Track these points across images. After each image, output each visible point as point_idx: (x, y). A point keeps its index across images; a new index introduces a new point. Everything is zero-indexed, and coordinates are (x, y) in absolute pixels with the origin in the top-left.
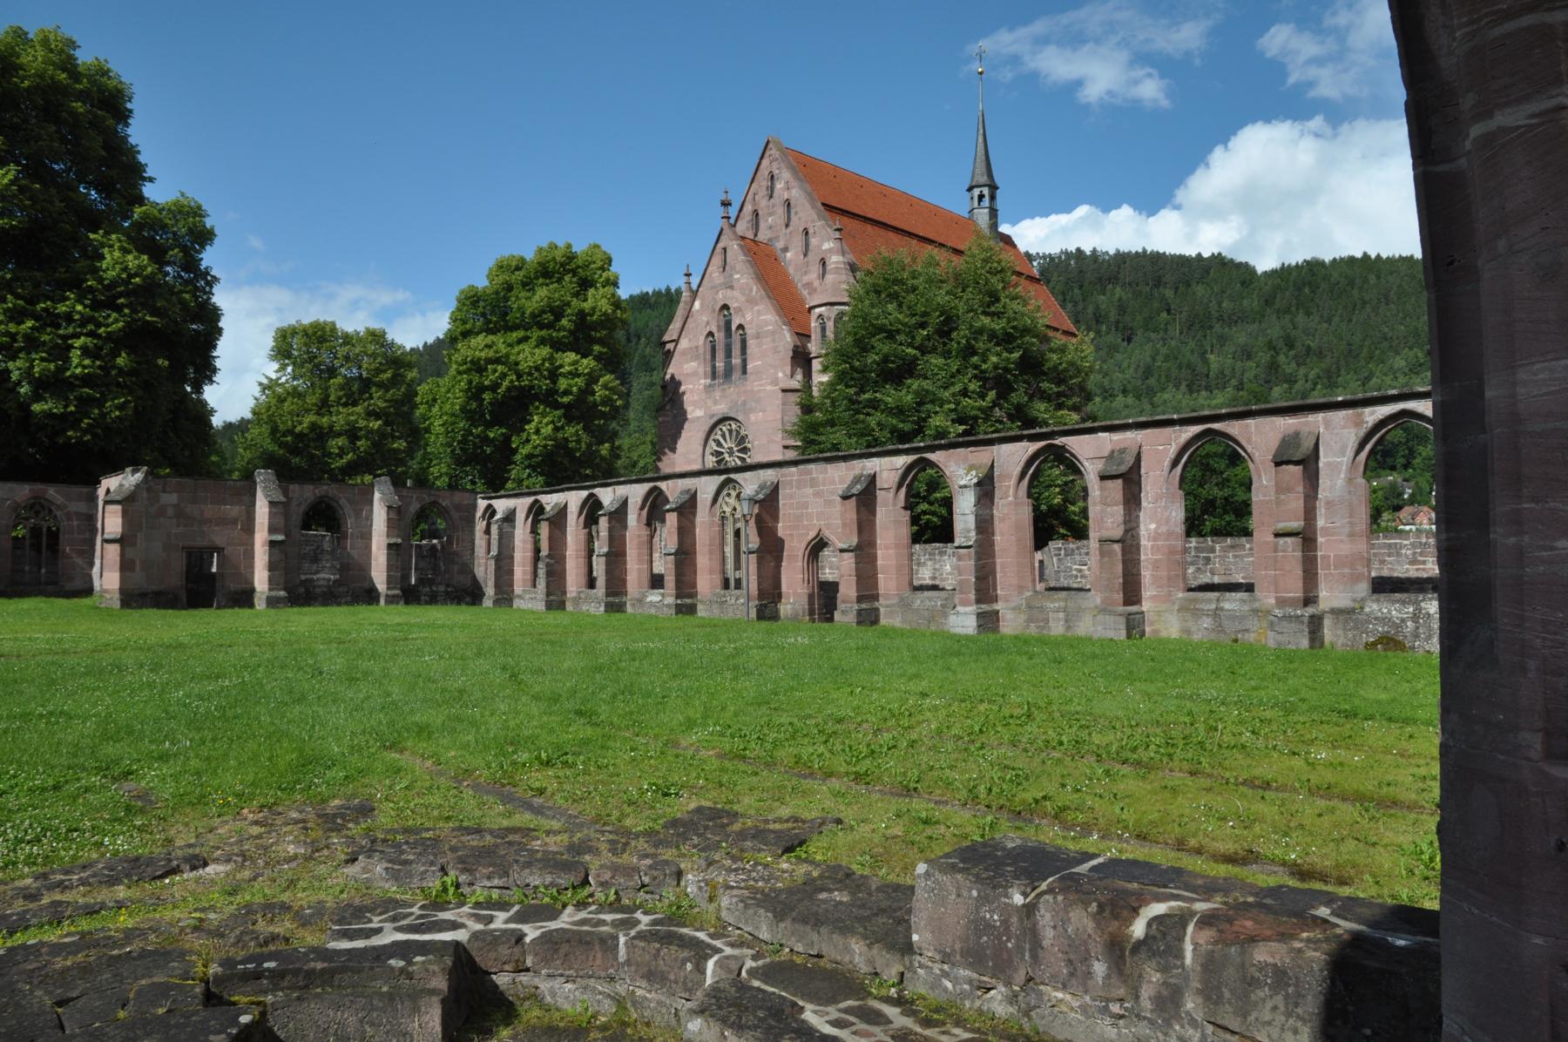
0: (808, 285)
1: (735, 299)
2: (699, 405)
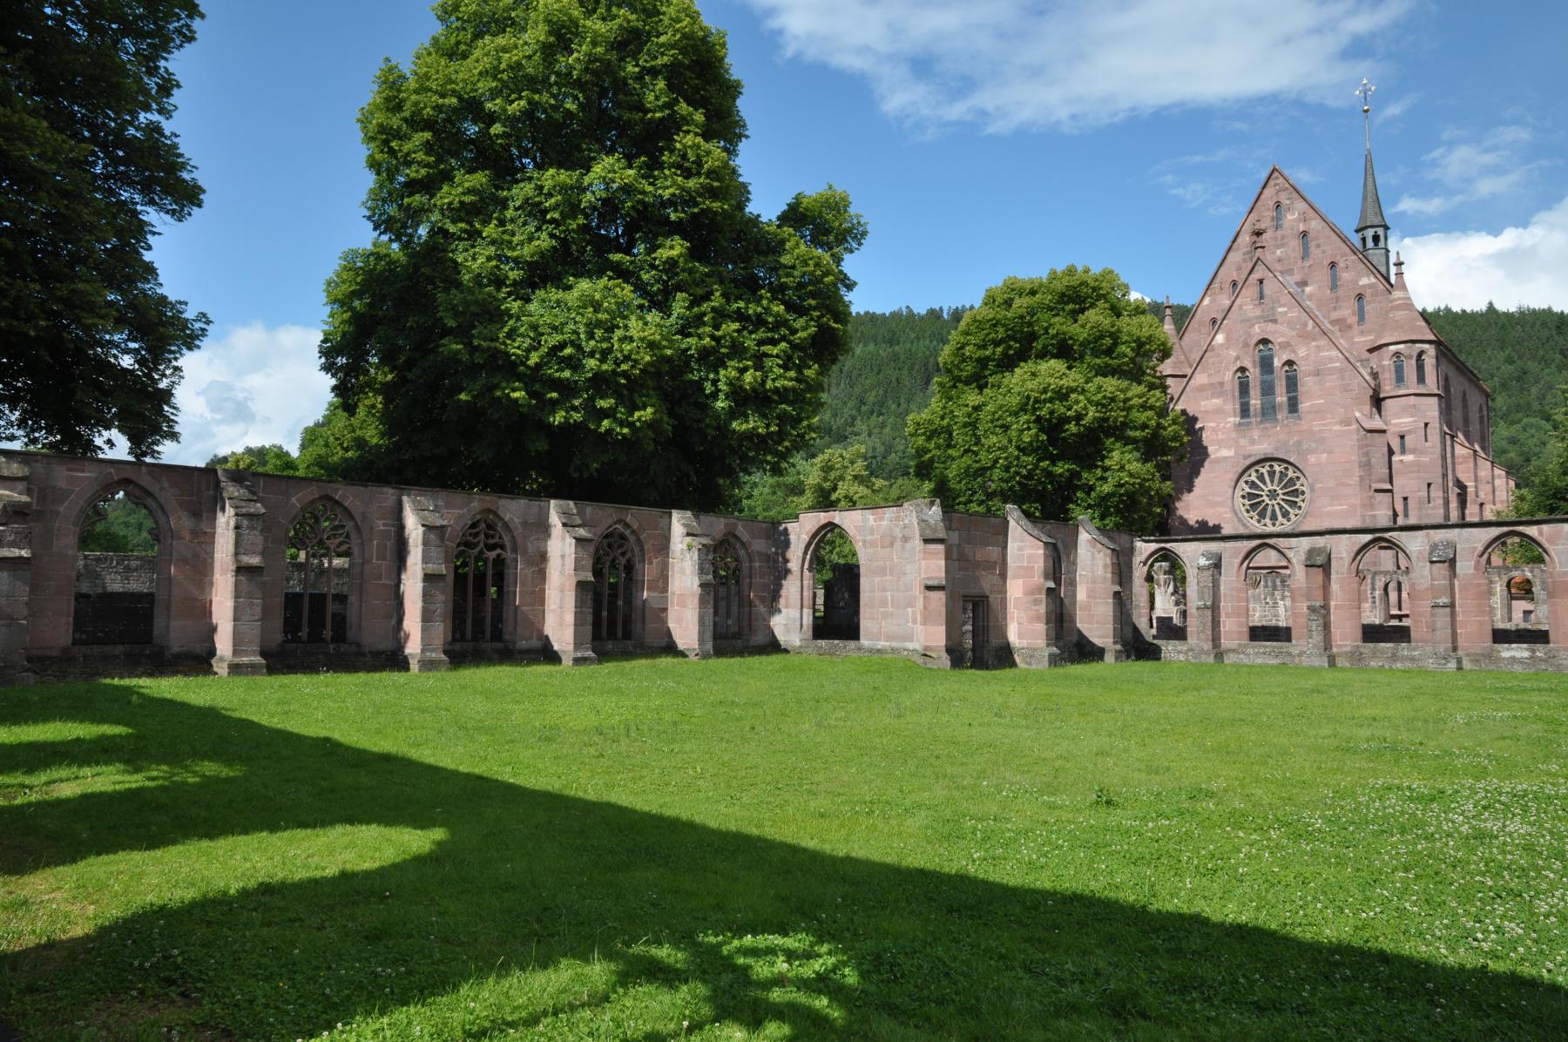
0: (1340, 323)
2: (1227, 442)
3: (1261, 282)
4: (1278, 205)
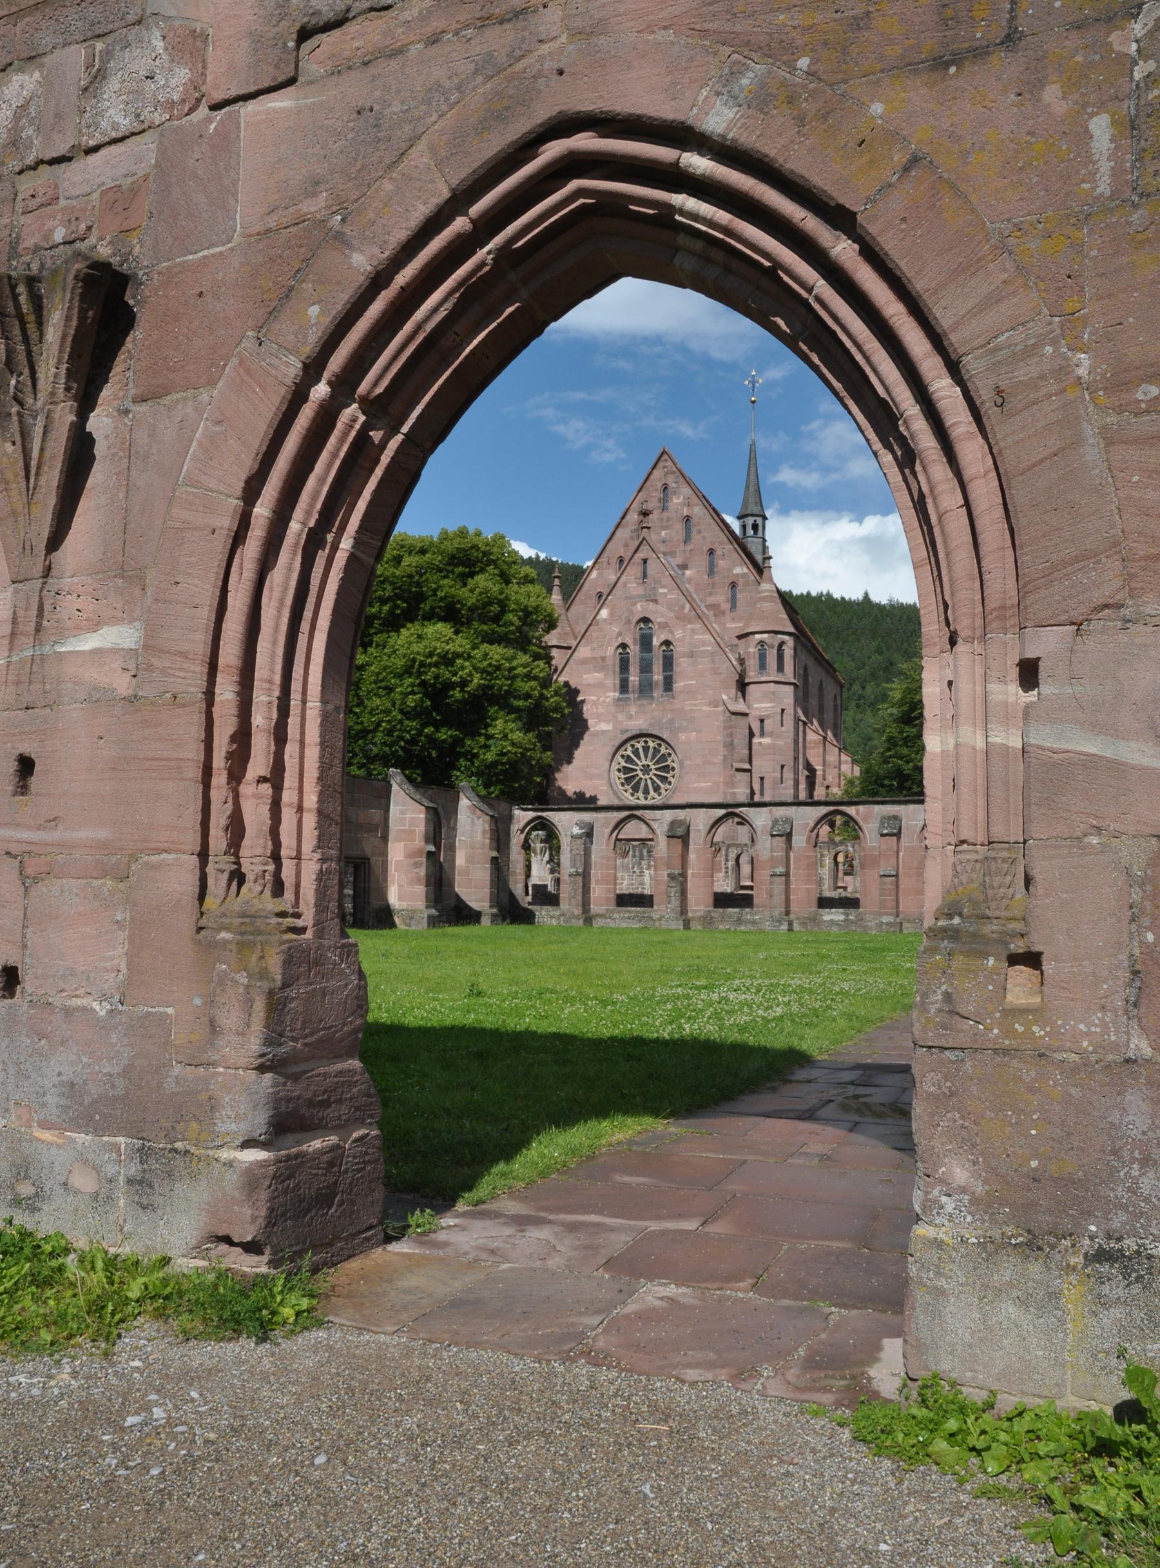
0: (713, 607)
1: (659, 614)
3: (645, 561)
4: (665, 488)
